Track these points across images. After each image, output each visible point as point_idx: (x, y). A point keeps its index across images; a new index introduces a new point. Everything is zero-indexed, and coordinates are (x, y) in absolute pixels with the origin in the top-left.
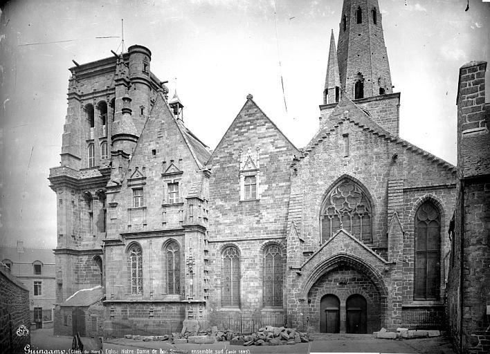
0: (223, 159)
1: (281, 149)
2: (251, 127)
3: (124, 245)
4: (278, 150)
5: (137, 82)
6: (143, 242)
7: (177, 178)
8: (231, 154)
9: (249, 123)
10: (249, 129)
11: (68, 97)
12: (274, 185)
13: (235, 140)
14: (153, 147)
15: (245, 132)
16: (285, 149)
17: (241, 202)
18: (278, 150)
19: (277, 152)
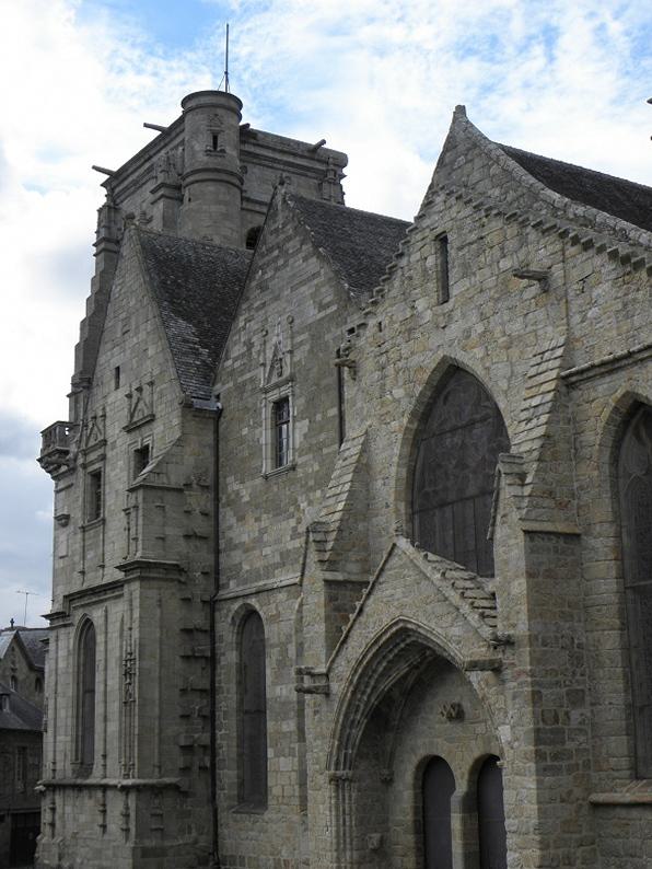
0: (237, 364)
1: (329, 311)
2: (281, 262)
3: (71, 625)
4: (322, 314)
5: (192, 183)
6: (97, 615)
7: (146, 431)
8: (250, 345)
9: (276, 253)
10: (277, 269)
11: (94, 250)
12: (319, 417)
13: (256, 305)
14: (115, 362)
15: (272, 278)
16: (334, 308)
17: (266, 477)
18: (322, 314)
19: (322, 319)
